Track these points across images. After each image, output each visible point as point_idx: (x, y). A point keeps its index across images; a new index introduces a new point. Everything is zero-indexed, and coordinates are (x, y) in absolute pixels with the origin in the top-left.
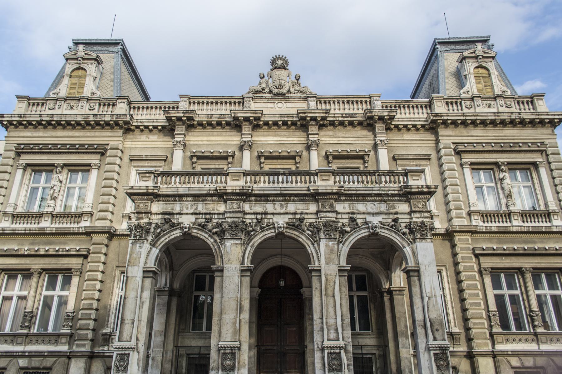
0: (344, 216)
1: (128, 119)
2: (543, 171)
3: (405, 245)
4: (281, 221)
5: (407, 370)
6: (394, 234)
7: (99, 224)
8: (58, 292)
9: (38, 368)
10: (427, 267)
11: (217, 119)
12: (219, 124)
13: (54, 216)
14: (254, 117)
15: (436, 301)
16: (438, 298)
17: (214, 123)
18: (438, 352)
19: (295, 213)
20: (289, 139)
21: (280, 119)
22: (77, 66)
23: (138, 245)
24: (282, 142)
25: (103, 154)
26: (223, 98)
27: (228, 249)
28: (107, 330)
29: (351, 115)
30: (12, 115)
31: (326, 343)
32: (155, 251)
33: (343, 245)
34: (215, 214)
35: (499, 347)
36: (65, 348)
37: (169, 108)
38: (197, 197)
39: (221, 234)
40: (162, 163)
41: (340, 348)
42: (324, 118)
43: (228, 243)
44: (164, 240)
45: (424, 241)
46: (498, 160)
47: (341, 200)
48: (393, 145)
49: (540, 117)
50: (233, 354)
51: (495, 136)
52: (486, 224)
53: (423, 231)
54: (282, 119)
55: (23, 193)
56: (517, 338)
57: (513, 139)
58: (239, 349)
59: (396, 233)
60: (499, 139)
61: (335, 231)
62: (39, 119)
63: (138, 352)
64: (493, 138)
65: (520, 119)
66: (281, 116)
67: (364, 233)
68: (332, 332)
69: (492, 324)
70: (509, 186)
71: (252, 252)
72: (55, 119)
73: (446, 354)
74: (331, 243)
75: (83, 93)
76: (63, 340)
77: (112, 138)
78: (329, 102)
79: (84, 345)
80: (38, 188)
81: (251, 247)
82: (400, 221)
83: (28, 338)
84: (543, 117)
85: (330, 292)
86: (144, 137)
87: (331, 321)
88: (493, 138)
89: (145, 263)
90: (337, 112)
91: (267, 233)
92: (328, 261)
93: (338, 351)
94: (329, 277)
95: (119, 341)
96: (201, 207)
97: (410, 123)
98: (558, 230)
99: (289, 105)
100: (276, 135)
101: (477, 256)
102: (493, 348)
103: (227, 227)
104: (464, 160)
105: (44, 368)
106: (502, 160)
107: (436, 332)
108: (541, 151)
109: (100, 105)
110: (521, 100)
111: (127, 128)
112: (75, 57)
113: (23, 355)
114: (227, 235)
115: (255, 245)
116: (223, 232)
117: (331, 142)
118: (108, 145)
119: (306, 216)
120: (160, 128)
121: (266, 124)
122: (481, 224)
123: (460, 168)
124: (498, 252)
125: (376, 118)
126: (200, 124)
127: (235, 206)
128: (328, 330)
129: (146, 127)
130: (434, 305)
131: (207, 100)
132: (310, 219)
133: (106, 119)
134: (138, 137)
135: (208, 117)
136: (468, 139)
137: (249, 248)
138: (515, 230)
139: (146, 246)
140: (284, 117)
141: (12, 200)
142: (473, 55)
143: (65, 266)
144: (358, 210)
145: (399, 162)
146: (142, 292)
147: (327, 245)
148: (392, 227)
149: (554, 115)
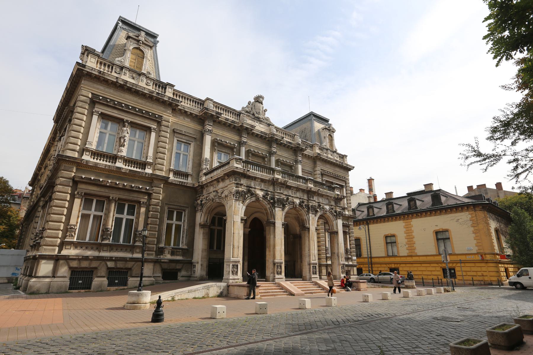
7: (158, 173)
8: (125, 216)
9: (122, 268)
13: (128, 161)
22: (136, 46)
26: (230, 108)
31: (312, 262)
36: (139, 256)
40: (193, 140)
43: (277, 209)
62: (115, 80)
66: (262, 132)
72: (128, 85)
76: (138, 251)
79: (152, 254)
80: (106, 133)
83: (111, 247)
86: (182, 118)
87: (313, 252)
99: (261, 126)
104: (324, 179)
105: (126, 269)
112: (137, 38)
113: (111, 259)
116: (274, 202)
129: (186, 112)
133: (165, 99)
134: (178, 116)
135: (226, 120)
139: (241, 205)
143: (135, 199)
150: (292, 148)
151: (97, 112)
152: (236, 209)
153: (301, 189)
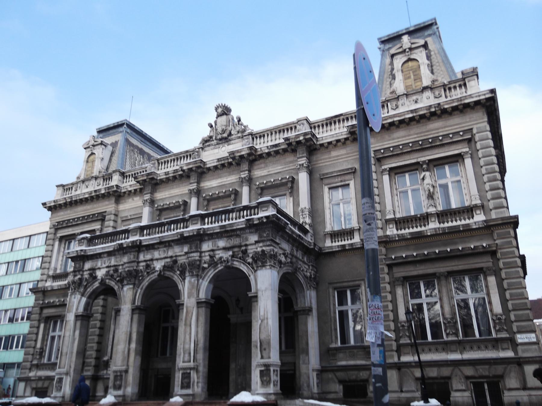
0: (207, 254)
1: (115, 189)
2: (468, 162)
3: (251, 273)
4: (158, 266)
5: (305, 385)
6: (242, 265)
10: (264, 292)
11: (171, 175)
12: (175, 178)
14: (196, 167)
15: (267, 323)
16: (269, 320)
17: (171, 178)
18: (263, 368)
19: (171, 257)
20: (228, 179)
21: (218, 163)
23: (73, 296)
24: (223, 183)
25: (103, 220)
27: (125, 293)
28: (106, 358)
29: (276, 146)
30: (50, 202)
32: (84, 300)
33: (203, 279)
34: (119, 265)
35: (405, 359)
37: (138, 173)
38: (110, 254)
39: (121, 281)
41: (191, 369)
42: (249, 155)
43: (125, 289)
44: (90, 290)
45: (264, 268)
46: (419, 160)
47: (205, 240)
48: (321, 165)
49: (463, 102)
50: (121, 376)
51: (417, 134)
52: (400, 232)
53: (264, 259)
54: (220, 163)
55: (60, 258)
56: (433, 348)
57: (438, 133)
58: (126, 371)
59: (244, 264)
60: (421, 136)
61: (196, 269)
63: (70, 376)
64: (416, 136)
65: (441, 110)
66: (219, 160)
67: (220, 267)
68: (187, 355)
69: (401, 335)
70: (428, 186)
71: (142, 293)
73: (270, 370)
74: (193, 280)
75: (92, 173)
77: (108, 207)
78: (264, 136)
81: (141, 289)
82: (249, 251)
84: (467, 101)
85: (188, 323)
86: (130, 200)
88: (416, 136)
89: (77, 309)
90: (262, 146)
91: (152, 276)
92: (193, 293)
93: (188, 371)
94: (189, 309)
95: (59, 368)
96: (113, 261)
97: (334, 139)
98: (477, 227)
100: (217, 178)
101: (390, 266)
102: (399, 359)
103: (125, 275)
104: (383, 167)
106: (423, 159)
107: (264, 352)
108: (469, 141)
109: (104, 180)
110: (452, 86)
111: (118, 195)
114: (125, 282)
115: (144, 288)
117: (263, 174)
118: (105, 212)
119: (179, 258)
120: (133, 191)
121: (209, 169)
122: (395, 232)
123: (379, 176)
124: (409, 259)
125: (294, 144)
126: (162, 181)
127: (132, 256)
128: (184, 354)
130: (265, 327)
131: (170, 158)
132: (182, 260)
134: (127, 201)
135: (166, 175)
136: (389, 144)
137: (139, 291)
138: (429, 234)
139: (78, 296)
140: (221, 161)
141: (53, 265)
142: (401, 50)
144: (218, 247)
145: (326, 181)
146: (74, 331)
147: (190, 282)
148: (240, 259)
149: (479, 96)
150: (285, 151)
151: (57, 238)
152: (71, 304)
153: (173, 241)
